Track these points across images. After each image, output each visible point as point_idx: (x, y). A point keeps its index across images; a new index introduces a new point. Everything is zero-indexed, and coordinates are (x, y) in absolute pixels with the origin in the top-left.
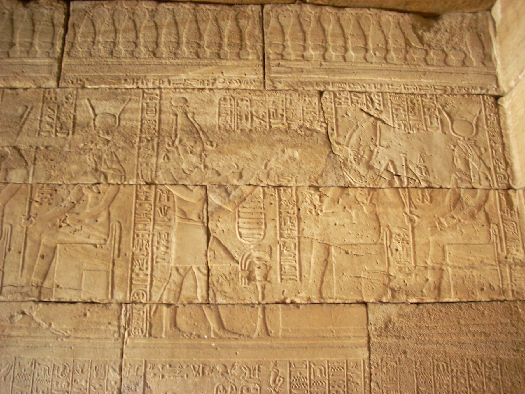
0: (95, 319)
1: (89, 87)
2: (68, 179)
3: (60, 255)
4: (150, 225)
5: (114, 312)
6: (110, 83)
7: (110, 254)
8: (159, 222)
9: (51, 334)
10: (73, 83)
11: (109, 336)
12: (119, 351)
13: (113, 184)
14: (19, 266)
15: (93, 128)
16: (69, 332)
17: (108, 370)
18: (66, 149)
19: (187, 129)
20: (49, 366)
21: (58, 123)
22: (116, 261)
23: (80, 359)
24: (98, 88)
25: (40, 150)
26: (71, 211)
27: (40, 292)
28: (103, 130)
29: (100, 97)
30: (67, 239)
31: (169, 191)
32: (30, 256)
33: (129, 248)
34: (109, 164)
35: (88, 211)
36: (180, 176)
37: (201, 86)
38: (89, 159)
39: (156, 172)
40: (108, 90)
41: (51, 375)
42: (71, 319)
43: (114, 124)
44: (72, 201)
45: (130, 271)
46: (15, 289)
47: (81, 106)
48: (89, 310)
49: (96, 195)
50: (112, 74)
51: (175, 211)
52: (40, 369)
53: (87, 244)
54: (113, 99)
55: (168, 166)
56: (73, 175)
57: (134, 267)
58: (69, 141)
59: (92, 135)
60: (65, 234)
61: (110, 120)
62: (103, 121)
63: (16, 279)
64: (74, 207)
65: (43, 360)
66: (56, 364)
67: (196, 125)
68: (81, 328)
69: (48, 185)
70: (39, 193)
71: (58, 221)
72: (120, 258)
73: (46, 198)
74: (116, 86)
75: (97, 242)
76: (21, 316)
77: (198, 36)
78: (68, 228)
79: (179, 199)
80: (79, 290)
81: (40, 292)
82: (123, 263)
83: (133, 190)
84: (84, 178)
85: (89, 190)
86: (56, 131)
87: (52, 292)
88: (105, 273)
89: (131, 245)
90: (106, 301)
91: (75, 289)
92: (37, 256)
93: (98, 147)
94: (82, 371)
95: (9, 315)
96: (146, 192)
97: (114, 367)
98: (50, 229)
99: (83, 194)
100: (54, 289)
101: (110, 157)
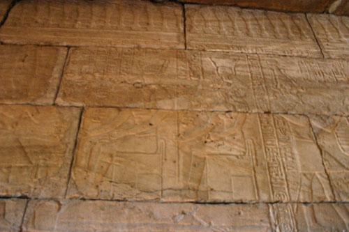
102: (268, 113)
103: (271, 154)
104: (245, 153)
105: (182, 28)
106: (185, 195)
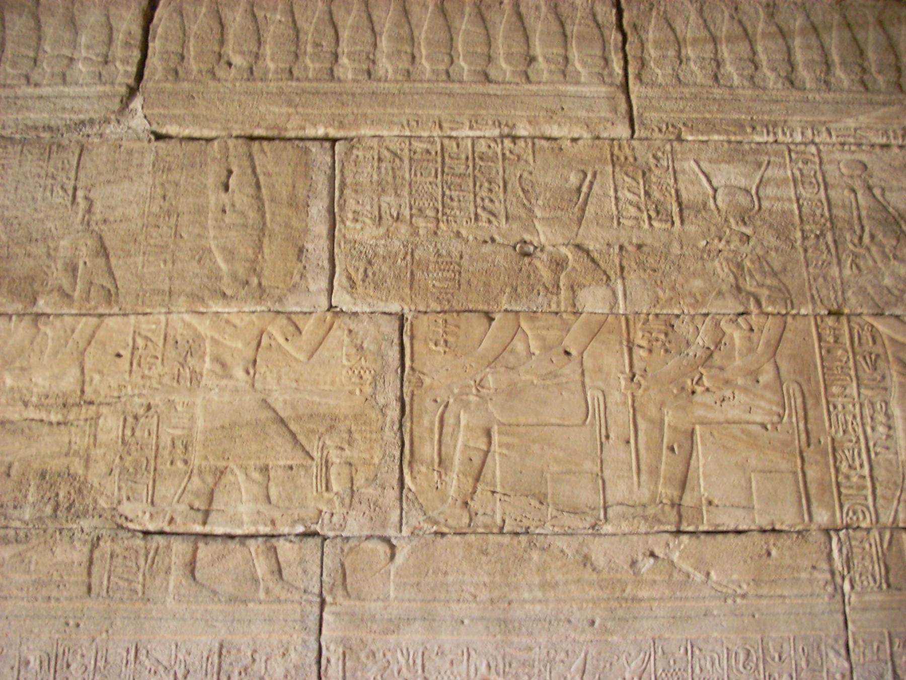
0: (788, 561)
1: (690, 138)
2: (692, 306)
3: (704, 445)
4: (851, 388)
5: (820, 546)
6: (727, 133)
7: (793, 440)
8: (866, 382)
9: (713, 592)
10: (660, 130)
11: (817, 591)
12: (841, 619)
13: (773, 315)
14: (631, 468)
15: (716, 212)
16: (745, 586)
17: (827, 654)
18: (676, 249)
19: (879, 216)
20: (719, 651)
21: (649, 203)
22: (805, 454)
23: (773, 635)
24: (707, 142)
25: (627, 251)
26: (708, 363)
27: (680, 515)
28: (734, 217)
29: (715, 156)
30: (711, 415)
31: (872, 326)
32: (648, 449)
33: (824, 429)
34: (758, 277)
35: (738, 362)
36: (885, 299)
37: (884, 141)
38: (721, 269)
39: (843, 293)
40: (726, 145)
41: (726, 667)
42: (745, 562)
43: (751, 206)
44: (706, 345)
45: (832, 470)
46: (631, 510)
47: (684, 171)
48: (774, 545)
49: (748, 334)
50: (727, 116)
51: (888, 362)
52: (701, 657)
53: (748, 423)
54: (739, 160)
55: (862, 281)
56: (699, 298)
57: (838, 463)
58: (677, 236)
59: (716, 225)
60: (705, 405)
61: (743, 200)
62: (730, 201)
63: (631, 492)
64: (711, 356)
65: (706, 641)
66: (730, 647)
67: (891, 209)
68: (766, 578)
69: (657, 315)
70: (643, 331)
71: (689, 382)
72: (812, 447)
73: (657, 340)
74: (739, 138)
75: (766, 419)
76: (652, 560)
77: (858, 53)
78: (708, 395)
79: (892, 340)
80: (749, 508)
81: (680, 515)
82: (818, 457)
83: (809, 324)
84: (720, 302)
85: (734, 326)
86: (650, 217)
87: (701, 513)
88: (791, 476)
89: (827, 424)
90: (799, 527)
91: (744, 507)
92: (661, 449)
93: (732, 247)
94: (780, 658)
95: (630, 561)
96: (835, 329)
97: (837, 647)
98: (676, 396)
99: (724, 333)
100: (704, 509)
101: (757, 266)
102: (836, 314)
103: (841, 416)
104: (781, 417)
105: (618, 69)
106: (655, 516)
